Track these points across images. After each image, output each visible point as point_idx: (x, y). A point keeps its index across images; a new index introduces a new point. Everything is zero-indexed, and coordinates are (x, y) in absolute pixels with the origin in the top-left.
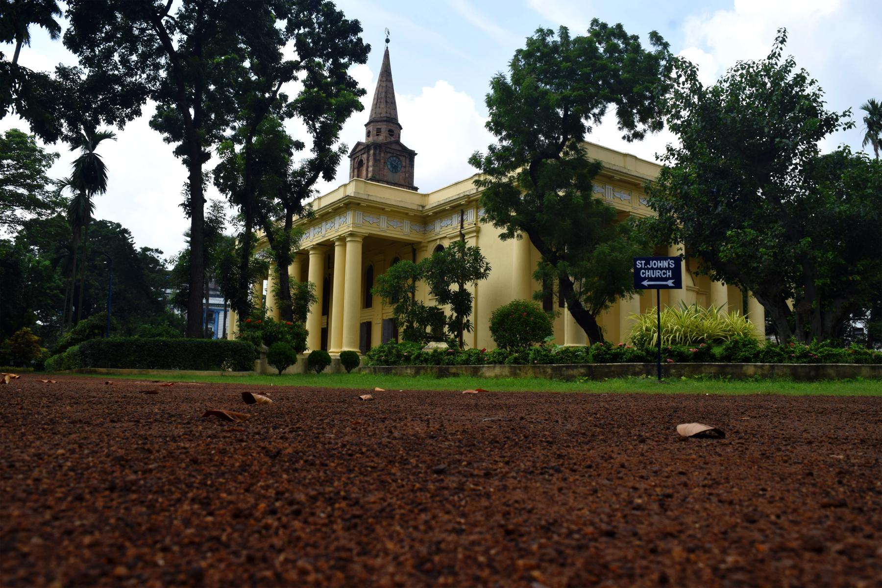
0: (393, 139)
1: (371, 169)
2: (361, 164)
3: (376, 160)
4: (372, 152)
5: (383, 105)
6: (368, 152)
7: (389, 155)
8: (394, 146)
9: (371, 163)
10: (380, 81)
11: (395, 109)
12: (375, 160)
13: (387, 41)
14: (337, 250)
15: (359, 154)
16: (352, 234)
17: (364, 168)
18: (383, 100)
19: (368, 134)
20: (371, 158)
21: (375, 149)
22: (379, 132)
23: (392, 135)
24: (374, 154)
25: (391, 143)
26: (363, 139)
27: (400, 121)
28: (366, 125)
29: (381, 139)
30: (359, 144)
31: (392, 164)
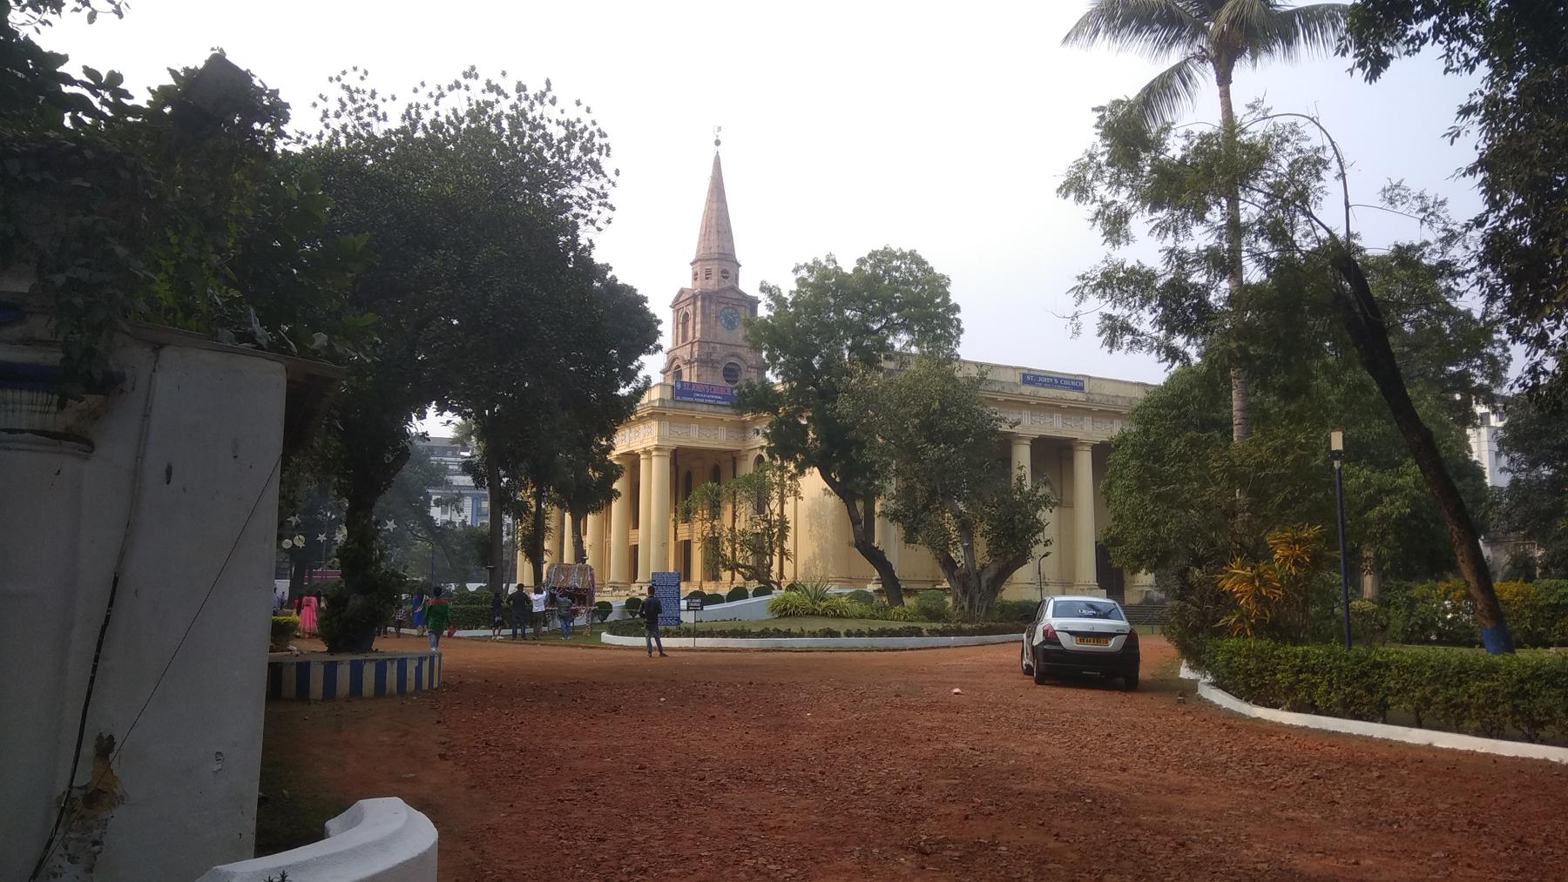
0: (728, 283)
1: (698, 327)
5: (714, 237)
8: (729, 294)
9: (698, 319)
10: (709, 201)
11: (730, 240)
12: (704, 314)
13: (718, 143)
14: (642, 463)
16: (657, 449)
17: (691, 323)
18: (714, 230)
20: (699, 311)
21: (703, 299)
22: (708, 274)
25: (724, 290)
26: (687, 282)
27: (739, 257)
29: (712, 285)
30: (682, 292)
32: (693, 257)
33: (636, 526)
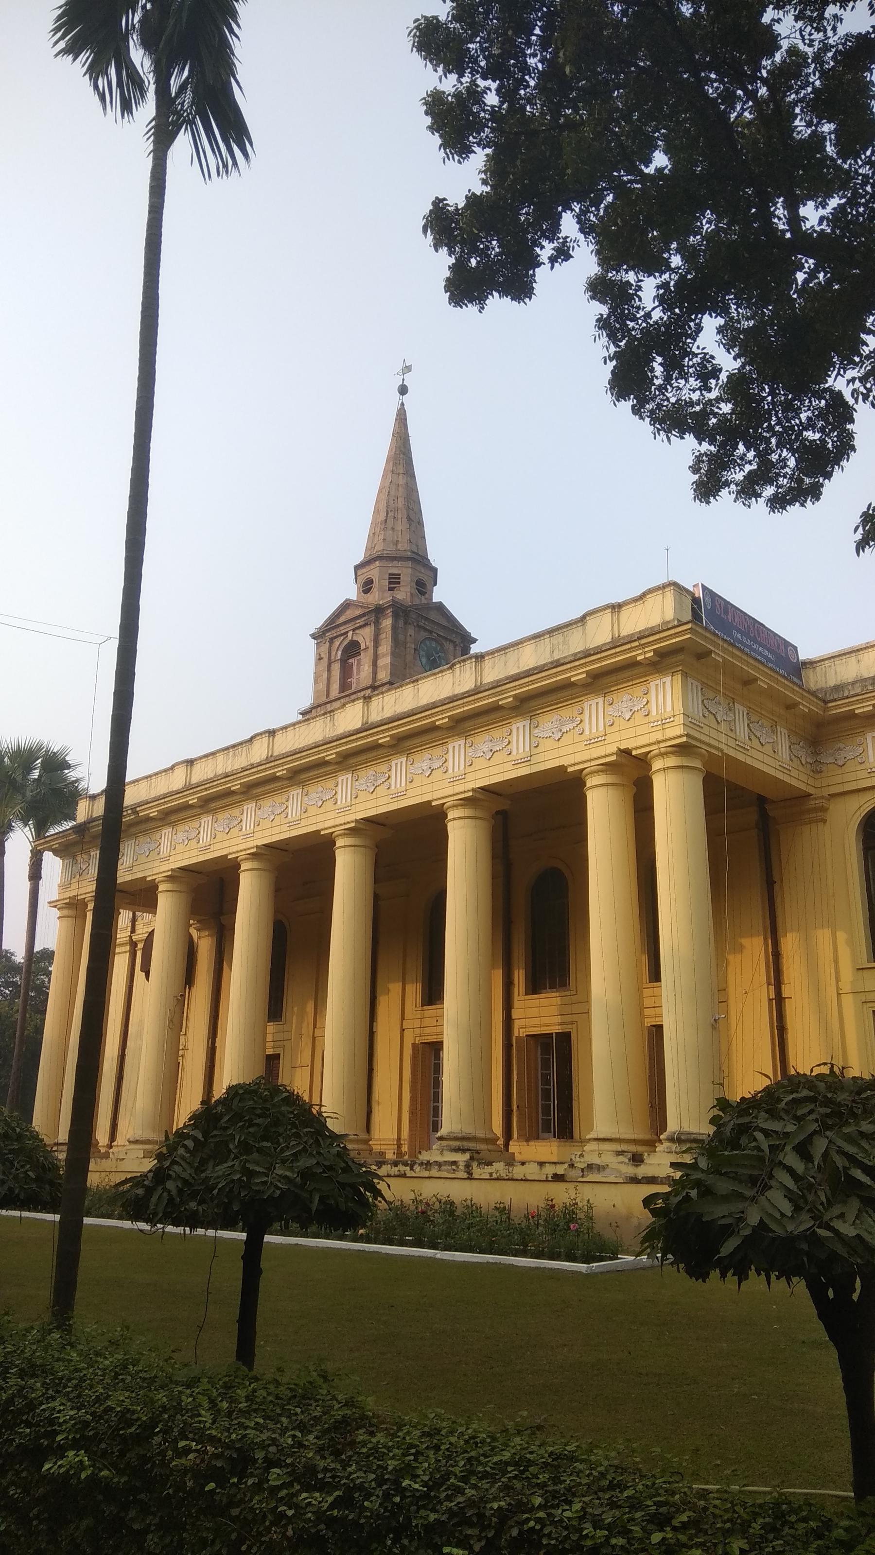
1: (385, 661)
2: (353, 649)
3: (397, 643)
4: (387, 623)
6: (377, 623)
7: (424, 634)
9: (385, 647)
15: (343, 630)
17: (366, 659)
18: (402, 515)
19: (367, 587)
21: (396, 616)
23: (423, 593)
24: (394, 628)
28: (357, 568)
31: (428, 657)
32: (360, 558)
33: (655, 975)
